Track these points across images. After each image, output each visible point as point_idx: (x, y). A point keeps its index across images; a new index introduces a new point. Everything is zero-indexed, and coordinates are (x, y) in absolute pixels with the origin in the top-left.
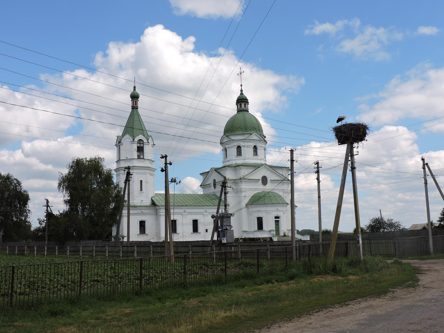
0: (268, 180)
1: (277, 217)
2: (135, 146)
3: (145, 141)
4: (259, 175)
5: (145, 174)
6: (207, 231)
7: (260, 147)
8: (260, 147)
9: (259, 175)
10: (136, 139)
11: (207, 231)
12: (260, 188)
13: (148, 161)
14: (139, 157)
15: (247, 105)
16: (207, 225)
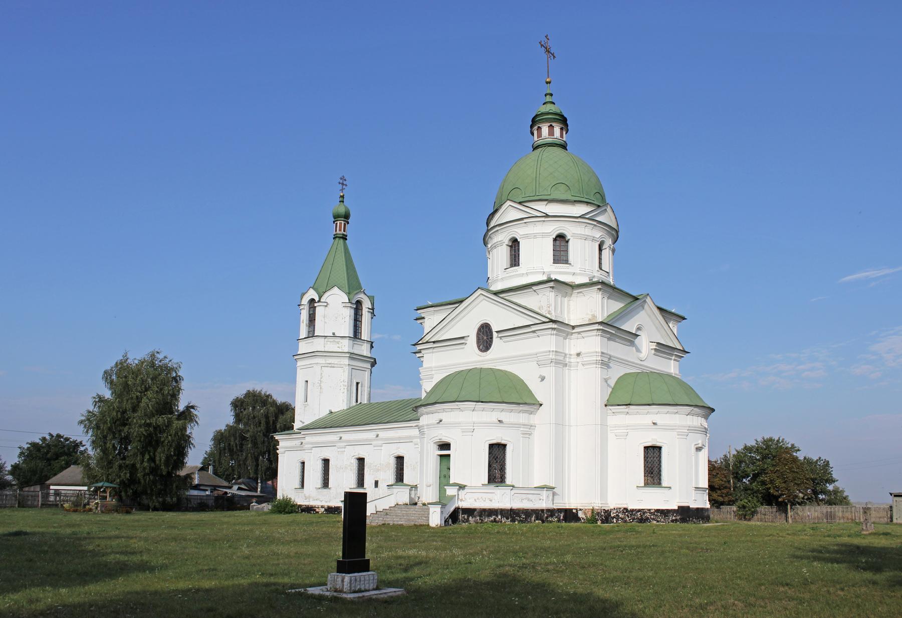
0: (495, 335)
1: (445, 446)
2: (304, 315)
3: (317, 300)
4: (466, 323)
5: (310, 366)
6: (376, 483)
7: (527, 236)
8: (527, 236)
9: (466, 323)
10: (305, 301)
11: (376, 483)
12: (469, 357)
13: (322, 340)
14: (311, 334)
15: (545, 130)
16: (378, 470)
